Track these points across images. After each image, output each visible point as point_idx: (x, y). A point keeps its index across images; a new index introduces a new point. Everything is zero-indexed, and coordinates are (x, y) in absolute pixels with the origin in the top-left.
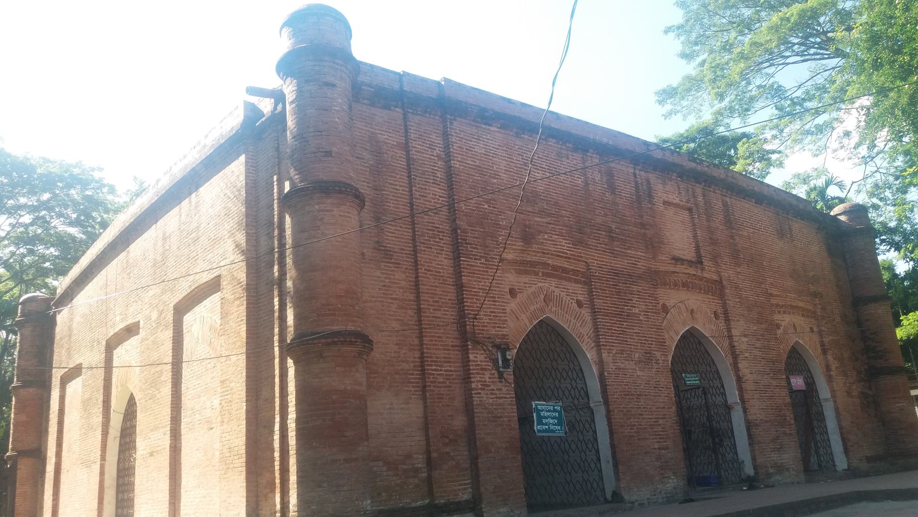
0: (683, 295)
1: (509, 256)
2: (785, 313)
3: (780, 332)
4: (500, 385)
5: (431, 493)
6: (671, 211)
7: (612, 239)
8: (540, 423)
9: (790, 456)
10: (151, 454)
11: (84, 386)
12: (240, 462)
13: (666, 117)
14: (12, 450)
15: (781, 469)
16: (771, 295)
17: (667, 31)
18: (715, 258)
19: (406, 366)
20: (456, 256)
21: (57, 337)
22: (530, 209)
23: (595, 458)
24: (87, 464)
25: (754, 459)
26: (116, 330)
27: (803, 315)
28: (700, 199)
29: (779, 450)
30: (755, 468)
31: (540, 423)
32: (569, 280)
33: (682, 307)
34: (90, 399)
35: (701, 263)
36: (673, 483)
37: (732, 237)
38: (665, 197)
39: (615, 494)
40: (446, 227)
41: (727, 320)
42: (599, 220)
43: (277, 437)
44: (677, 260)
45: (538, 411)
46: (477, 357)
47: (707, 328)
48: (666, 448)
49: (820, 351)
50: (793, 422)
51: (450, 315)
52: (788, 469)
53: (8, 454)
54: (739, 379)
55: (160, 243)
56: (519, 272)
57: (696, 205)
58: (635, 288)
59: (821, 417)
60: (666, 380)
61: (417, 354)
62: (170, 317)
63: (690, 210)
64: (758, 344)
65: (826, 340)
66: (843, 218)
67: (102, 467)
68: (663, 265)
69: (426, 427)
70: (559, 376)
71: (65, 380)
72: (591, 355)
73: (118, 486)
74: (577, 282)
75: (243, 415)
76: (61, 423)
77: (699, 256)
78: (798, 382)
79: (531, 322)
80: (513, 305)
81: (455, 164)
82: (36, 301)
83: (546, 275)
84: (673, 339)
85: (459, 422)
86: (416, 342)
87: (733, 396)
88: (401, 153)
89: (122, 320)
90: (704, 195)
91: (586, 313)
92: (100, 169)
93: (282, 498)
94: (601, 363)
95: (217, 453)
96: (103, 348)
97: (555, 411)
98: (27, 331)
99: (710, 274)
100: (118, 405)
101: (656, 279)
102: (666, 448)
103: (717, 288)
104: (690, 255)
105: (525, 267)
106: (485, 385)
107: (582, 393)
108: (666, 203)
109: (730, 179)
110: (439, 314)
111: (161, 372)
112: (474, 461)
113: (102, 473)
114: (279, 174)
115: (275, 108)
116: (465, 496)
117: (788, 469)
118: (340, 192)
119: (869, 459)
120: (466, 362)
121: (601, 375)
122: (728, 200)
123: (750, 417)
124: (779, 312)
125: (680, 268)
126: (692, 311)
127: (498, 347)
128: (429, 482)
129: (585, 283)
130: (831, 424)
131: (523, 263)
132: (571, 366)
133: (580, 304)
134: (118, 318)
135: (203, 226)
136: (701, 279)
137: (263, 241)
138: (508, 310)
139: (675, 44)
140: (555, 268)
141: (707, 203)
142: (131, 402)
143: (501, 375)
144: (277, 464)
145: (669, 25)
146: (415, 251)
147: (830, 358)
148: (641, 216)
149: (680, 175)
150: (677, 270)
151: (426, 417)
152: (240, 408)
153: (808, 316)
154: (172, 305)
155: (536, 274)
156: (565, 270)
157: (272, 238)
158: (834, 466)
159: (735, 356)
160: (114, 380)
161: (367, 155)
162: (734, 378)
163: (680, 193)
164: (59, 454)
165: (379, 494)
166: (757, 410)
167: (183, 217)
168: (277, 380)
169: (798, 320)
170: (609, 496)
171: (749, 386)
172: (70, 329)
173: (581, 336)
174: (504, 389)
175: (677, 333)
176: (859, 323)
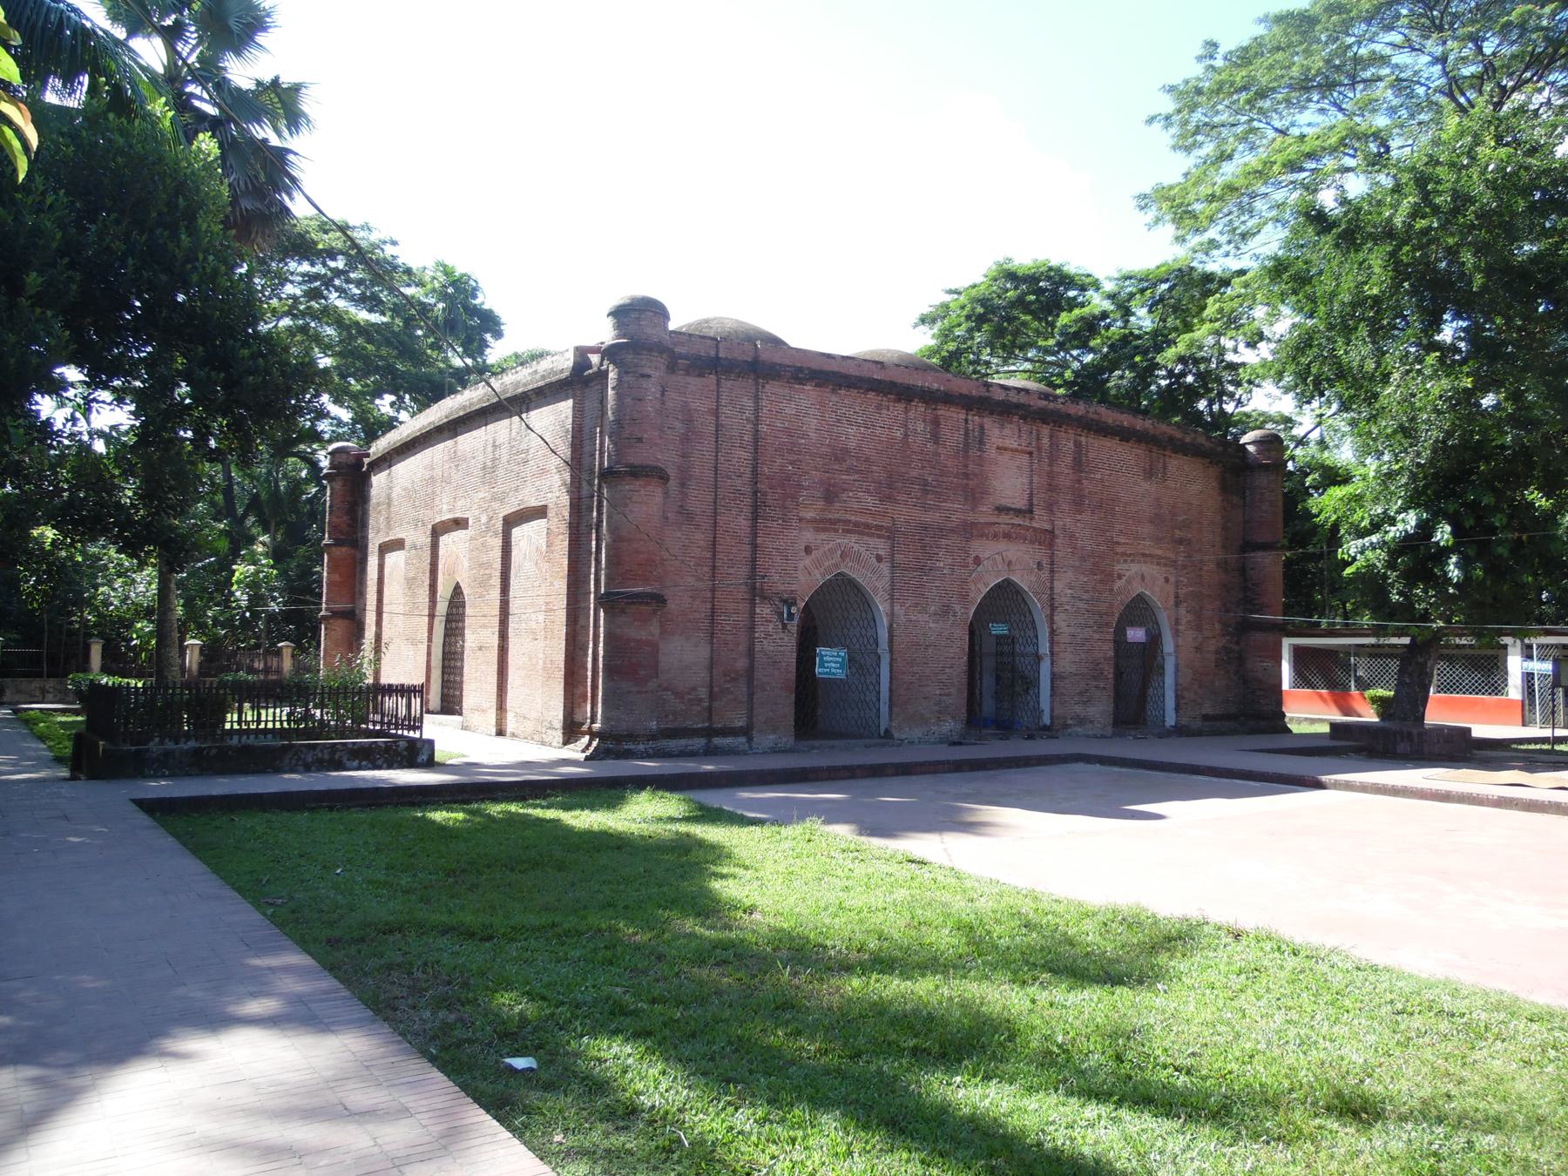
0: (1002, 545)
1: (809, 515)
2: (1132, 561)
3: (1118, 584)
4: (782, 635)
5: (710, 719)
6: (1007, 455)
7: (926, 492)
8: (822, 666)
9: (1100, 709)
10: (480, 649)
11: (407, 563)
12: (560, 674)
13: (1150, 227)
14: (327, 609)
15: (1082, 721)
16: (1118, 543)
17: (1151, 120)
18: (1050, 507)
19: (697, 616)
20: (755, 518)
21: (373, 501)
22: (836, 467)
23: (874, 699)
24: (414, 642)
25: (1052, 710)
26: (444, 518)
27: (1158, 564)
28: (1045, 441)
29: (1084, 703)
30: (1052, 718)
31: (822, 666)
32: (872, 535)
33: (998, 558)
34: (414, 578)
35: (1031, 512)
36: (950, 726)
37: (1079, 482)
38: (1000, 443)
39: (887, 731)
40: (748, 489)
41: (1052, 571)
42: (914, 473)
43: (590, 659)
44: (1001, 510)
45: (822, 656)
46: (764, 610)
47: (1022, 580)
48: (949, 695)
49: (1172, 601)
50: (1111, 676)
51: (744, 571)
52: (1091, 722)
53: (322, 613)
54: (1052, 632)
55: (490, 449)
56: (818, 530)
57: (1039, 449)
58: (944, 542)
59: (1161, 671)
60: (962, 635)
61: (709, 606)
62: (499, 525)
63: (1030, 453)
64: (1085, 596)
65: (1182, 592)
66: (1251, 448)
67: (429, 647)
68: (984, 514)
69: (711, 666)
70: (848, 624)
71: (385, 549)
72: (882, 607)
73: (443, 667)
74: (879, 537)
75: (563, 637)
76: (380, 592)
77: (1031, 504)
78: (1136, 634)
79: (823, 575)
80: (807, 561)
81: (763, 428)
82: (348, 453)
83: (844, 531)
84: (979, 592)
85: (742, 664)
86: (709, 595)
87: (1044, 648)
88: (712, 419)
89: (450, 511)
90: (1051, 437)
91: (885, 568)
92: (394, 243)
93: (592, 709)
94: (892, 615)
95: (541, 662)
96: (429, 532)
97: (838, 656)
98: (338, 485)
99: (1040, 522)
100: (444, 591)
101: (970, 530)
102: (949, 695)
103: (1047, 538)
104: (1021, 503)
105: (823, 525)
106: (768, 635)
107: (871, 641)
108: (998, 448)
109: (1091, 415)
110: (731, 571)
111: (490, 576)
112: (751, 695)
113: (429, 654)
114: (601, 426)
115: (601, 365)
116: (740, 723)
117: (1091, 722)
118: (647, 476)
119: (1206, 718)
120: (753, 614)
121: (891, 626)
122: (1083, 439)
123: (1056, 670)
124: (1125, 561)
125: (1004, 518)
126: (1010, 563)
127: (785, 602)
128: (710, 709)
129: (889, 538)
130: (1169, 679)
131: (822, 521)
132: (864, 615)
133: (879, 559)
134: (445, 507)
135: (532, 451)
136: (1028, 529)
137: (585, 485)
138: (801, 566)
139: (1164, 137)
140: (857, 524)
141: (1054, 445)
142: (457, 590)
143: (784, 626)
144: (589, 680)
145: (1153, 114)
146: (715, 513)
147: (1182, 611)
148: (966, 466)
149: (1024, 418)
150: (1000, 521)
151: (712, 658)
152: (561, 616)
153: (1165, 565)
154: (501, 515)
155: (836, 531)
156: (868, 526)
157: (593, 485)
158: (1164, 721)
159: (1053, 608)
160: (440, 567)
161: (677, 424)
162: (1047, 630)
163: (1020, 437)
164: (379, 623)
165: (666, 716)
166: (1067, 663)
167: (514, 434)
168: (592, 612)
169: (1150, 570)
170: (882, 734)
171: (1063, 638)
172: (389, 497)
173: (875, 589)
174: (786, 639)
175: (986, 585)
176: (1243, 570)
